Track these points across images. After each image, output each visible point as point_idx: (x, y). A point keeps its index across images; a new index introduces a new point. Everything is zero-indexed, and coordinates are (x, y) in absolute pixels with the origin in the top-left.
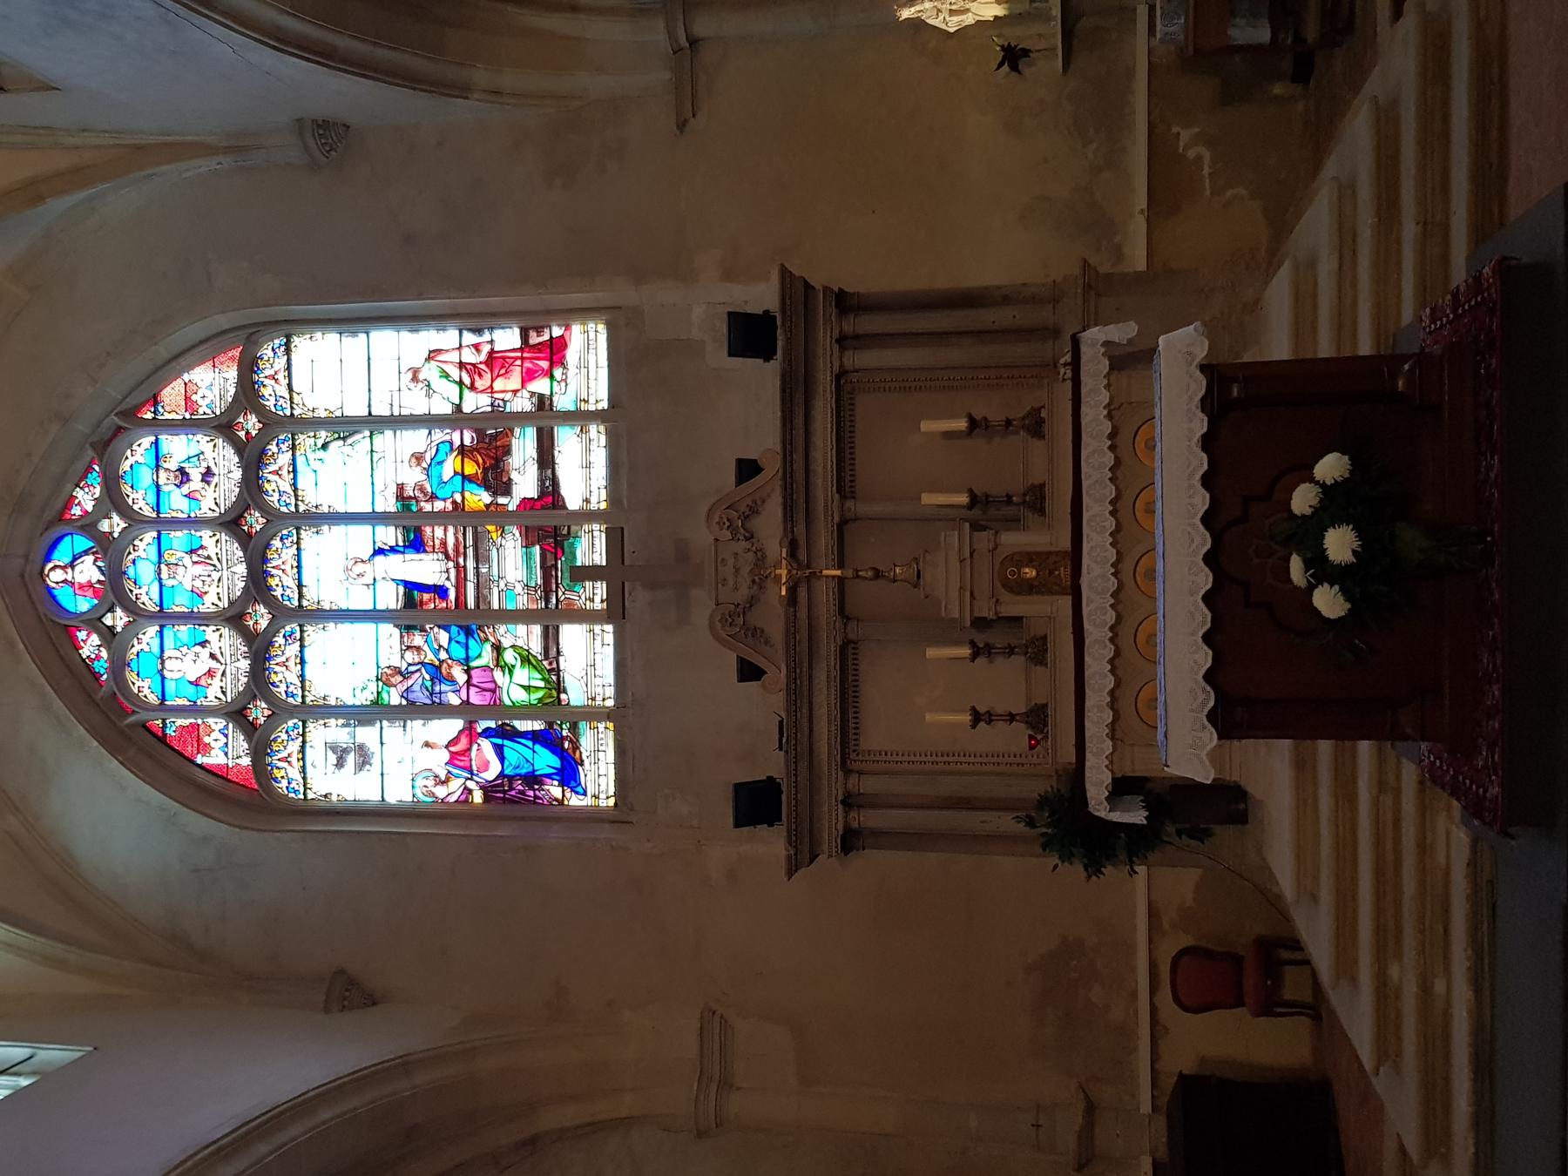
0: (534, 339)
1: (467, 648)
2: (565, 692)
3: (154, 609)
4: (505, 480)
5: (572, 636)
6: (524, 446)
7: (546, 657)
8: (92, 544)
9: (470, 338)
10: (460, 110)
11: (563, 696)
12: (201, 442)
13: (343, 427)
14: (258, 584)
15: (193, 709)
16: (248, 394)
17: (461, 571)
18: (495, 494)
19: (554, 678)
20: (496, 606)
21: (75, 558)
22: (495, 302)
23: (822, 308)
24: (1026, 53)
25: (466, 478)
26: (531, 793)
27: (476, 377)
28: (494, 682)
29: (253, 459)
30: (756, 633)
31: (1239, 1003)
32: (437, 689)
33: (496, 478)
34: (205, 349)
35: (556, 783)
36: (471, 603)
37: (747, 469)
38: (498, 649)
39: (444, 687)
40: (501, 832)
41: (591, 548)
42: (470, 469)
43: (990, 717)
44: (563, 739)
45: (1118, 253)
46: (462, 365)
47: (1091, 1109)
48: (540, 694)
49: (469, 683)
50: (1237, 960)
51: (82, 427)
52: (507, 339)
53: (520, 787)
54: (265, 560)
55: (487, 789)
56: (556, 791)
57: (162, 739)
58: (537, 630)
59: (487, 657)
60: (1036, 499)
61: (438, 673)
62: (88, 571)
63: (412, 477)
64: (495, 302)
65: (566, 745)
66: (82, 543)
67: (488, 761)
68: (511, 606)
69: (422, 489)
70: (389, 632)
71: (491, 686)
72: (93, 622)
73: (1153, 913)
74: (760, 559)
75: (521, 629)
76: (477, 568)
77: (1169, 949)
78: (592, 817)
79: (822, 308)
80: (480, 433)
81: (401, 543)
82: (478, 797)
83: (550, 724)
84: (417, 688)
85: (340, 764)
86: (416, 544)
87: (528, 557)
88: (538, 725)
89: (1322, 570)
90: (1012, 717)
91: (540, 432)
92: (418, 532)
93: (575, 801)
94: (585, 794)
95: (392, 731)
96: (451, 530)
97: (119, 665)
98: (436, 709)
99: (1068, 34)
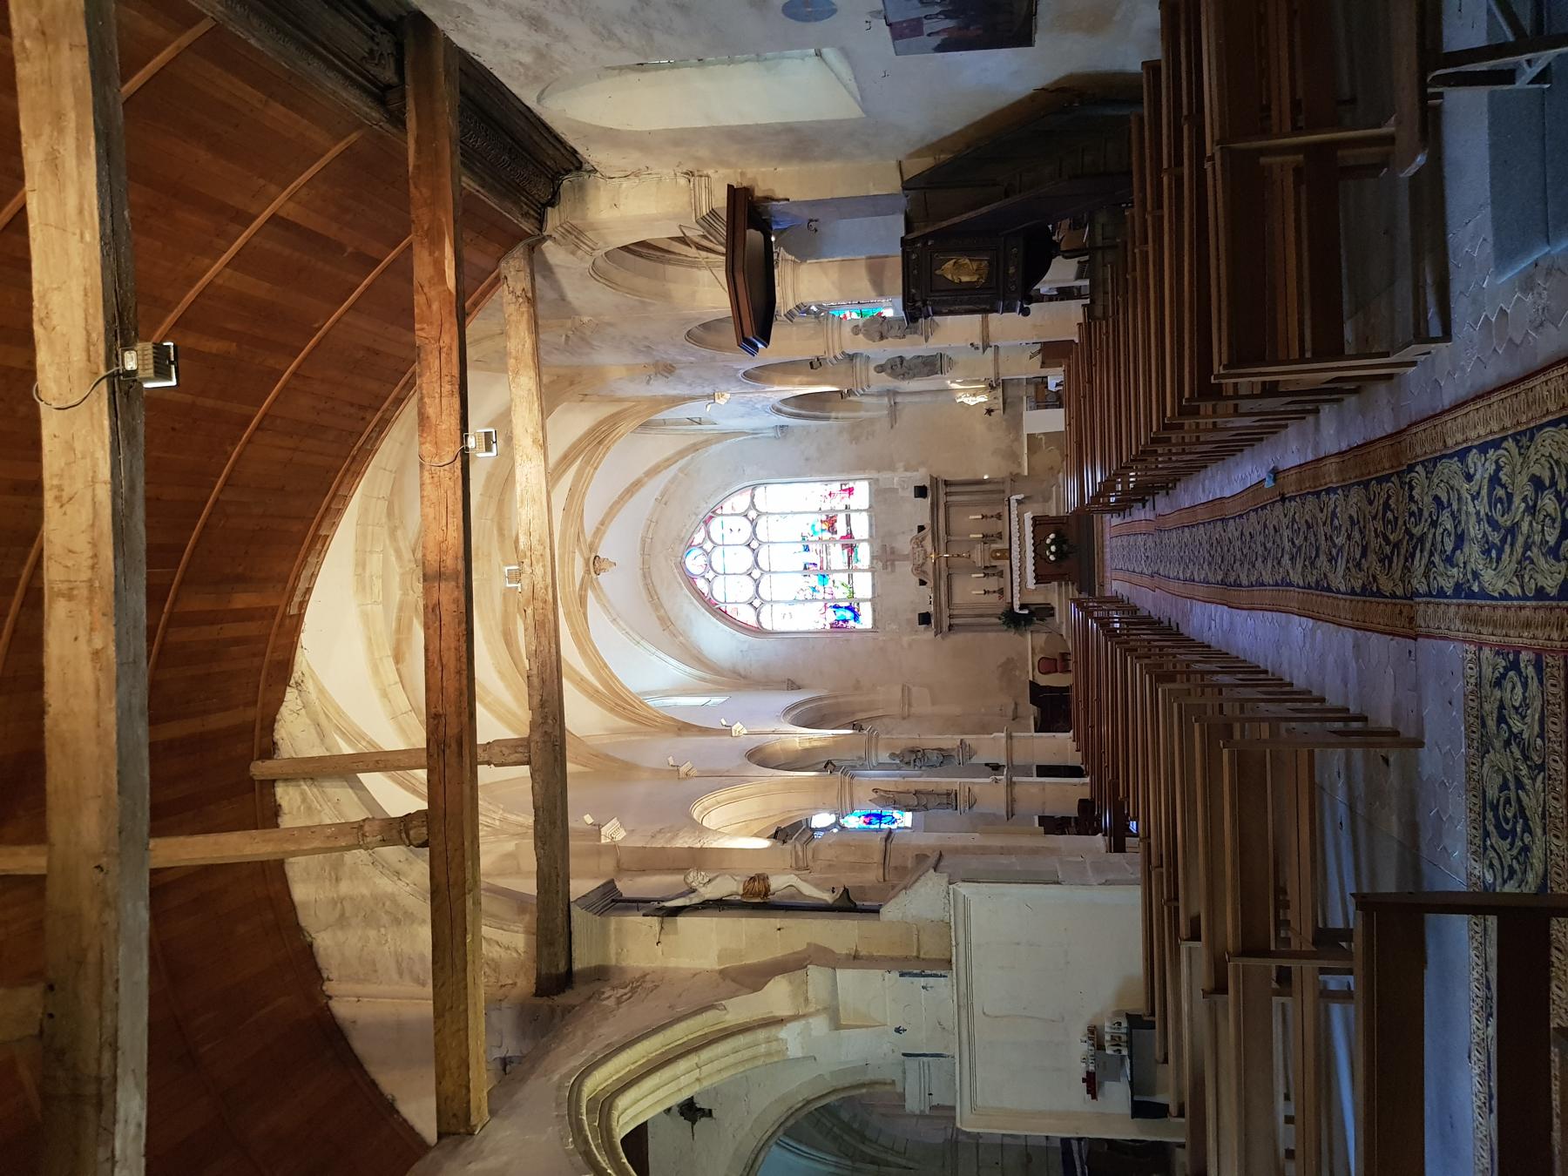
0: (844, 487)
6: (841, 519)
16: (753, 504)
22: (833, 478)
23: (941, 486)
24: (992, 411)
25: (823, 530)
29: (754, 523)
30: (924, 572)
31: (1056, 671)
33: (832, 529)
37: (921, 528)
40: (839, 635)
41: (864, 553)
42: (825, 527)
43: (989, 592)
45: (1020, 465)
47: (1016, 704)
50: (1056, 660)
51: (701, 517)
52: (835, 487)
56: (852, 623)
59: (831, 582)
60: (1000, 536)
62: (702, 560)
63: (807, 531)
64: (833, 478)
67: (831, 617)
70: (800, 576)
73: (1033, 649)
74: (925, 552)
75: (841, 574)
77: (1037, 659)
79: (941, 486)
82: (828, 627)
86: (807, 549)
88: (847, 604)
89: (1052, 553)
90: (994, 592)
93: (858, 626)
95: (798, 606)
99: (1004, 403)
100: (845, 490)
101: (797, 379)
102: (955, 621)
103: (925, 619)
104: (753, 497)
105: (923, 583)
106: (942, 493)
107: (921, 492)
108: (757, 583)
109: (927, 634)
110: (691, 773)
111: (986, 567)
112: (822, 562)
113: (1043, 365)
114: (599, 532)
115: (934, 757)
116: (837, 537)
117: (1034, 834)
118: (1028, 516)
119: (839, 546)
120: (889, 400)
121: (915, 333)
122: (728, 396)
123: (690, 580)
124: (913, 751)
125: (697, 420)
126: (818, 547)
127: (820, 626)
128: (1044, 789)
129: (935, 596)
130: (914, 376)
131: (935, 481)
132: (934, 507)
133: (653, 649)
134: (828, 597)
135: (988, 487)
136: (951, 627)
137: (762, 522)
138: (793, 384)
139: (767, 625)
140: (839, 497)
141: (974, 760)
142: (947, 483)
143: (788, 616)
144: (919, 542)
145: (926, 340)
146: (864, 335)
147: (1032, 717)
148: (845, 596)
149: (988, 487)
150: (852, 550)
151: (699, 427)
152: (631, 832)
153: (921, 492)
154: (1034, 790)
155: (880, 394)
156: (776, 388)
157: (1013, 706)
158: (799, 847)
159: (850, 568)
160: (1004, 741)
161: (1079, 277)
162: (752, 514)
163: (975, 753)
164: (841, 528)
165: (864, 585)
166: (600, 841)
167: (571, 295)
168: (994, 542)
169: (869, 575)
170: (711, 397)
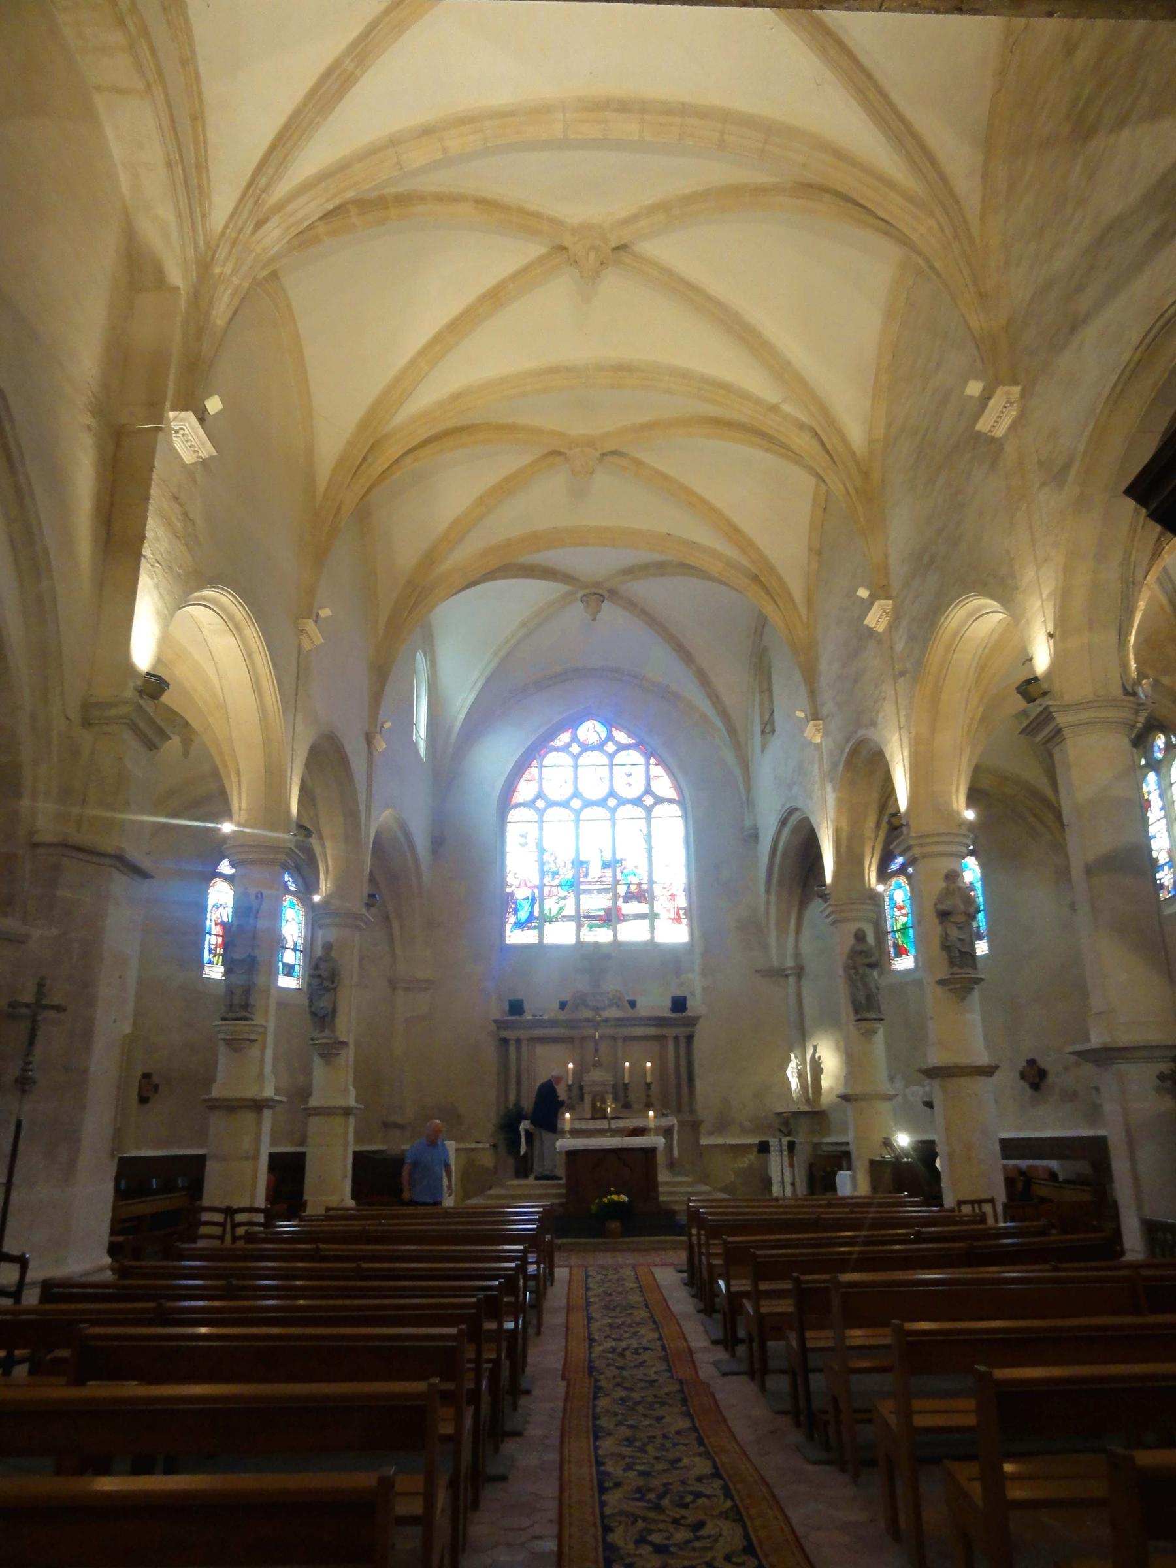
0: (681, 912)
1: (565, 885)
2: (550, 924)
3: (579, 763)
4: (629, 900)
5: (572, 925)
6: (643, 908)
7: (562, 917)
8: (603, 739)
9: (682, 887)
10: (762, 889)
11: (548, 923)
12: (643, 782)
13: (648, 838)
14: (588, 804)
15: (541, 779)
16: (659, 800)
17: (594, 883)
18: (624, 897)
19: (554, 919)
20: (581, 896)
21: (598, 732)
26: (511, 910)
27: (667, 889)
28: (553, 896)
29: (637, 802)
32: (550, 873)
33: (629, 897)
34: (677, 786)
35: (515, 920)
36: (582, 887)
38: (565, 898)
39: (550, 876)
41: (603, 936)
42: (633, 887)
44: (531, 923)
45: (711, 1134)
46: (671, 884)
47: (401, 1127)
48: (548, 914)
49: (552, 886)
52: (682, 901)
53: (513, 906)
54: (598, 806)
55: (512, 894)
57: (530, 766)
58: (573, 913)
59: (563, 894)
61: (556, 874)
62: (593, 739)
63: (628, 865)
64: (694, 898)
65: (529, 924)
66: (604, 735)
67: (521, 894)
68: (581, 902)
69: (625, 868)
70: (572, 856)
71: (551, 895)
72: (574, 739)
74: (604, 1009)
76: (595, 890)
78: (502, 935)
80: (646, 891)
81: (605, 860)
82: (508, 890)
83: (537, 918)
84: (550, 866)
85: (522, 836)
86: (606, 865)
87: (600, 910)
88: (536, 914)
91: (647, 914)
92: (609, 866)
93: (508, 927)
94: (511, 932)
95: (535, 856)
96: (610, 879)
97: (557, 749)
98: (543, 874)
100: (678, 914)
101: (845, 825)
102: (512, 1049)
103: (516, 1008)
104: (670, 801)
105: (563, 1005)
106: (681, 1031)
107: (679, 1004)
108: (565, 804)
109: (497, 1010)
110: (304, 638)
111: (581, 1088)
112: (590, 883)
113: (874, 1164)
114: (631, 605)
115: (324, 1003)
116: (620, 903)
117: (118, 1134)
118: (660, 1141)
119: (609, 904)
120: (791, 968)
121: (952, 964)
122: (817, 740)
123: (572, 723)
124: (334, 975)
125: (768, 729)
126: (608, 880)
127: (510, 879)
128: (247, 1158)
129: (546, 1021)
130: (851, 981)
131: (693, 1022)
132: (660, 1022)
133: (487, 673)
134: (546, 890)
135: (685, 1091)
136: (505, 1042)
137: (639, 812)
138: (837, 821)
139: (513, 815)
140: (670, 905)
141: (317, 1060)
142: (690, 1038)
143: (523, 840)
144: (616, 1002)
145: (942, 982)
146: (947, 889)
147: (385, 1147)
148: (547, 912)
149: (685, 1091)
150: (605, 921)
151: (758, 728)
152: (189, 471)
153: (679, 1004)
154: (247, 1143)
155: (797, 955)
156: (831, 797)
157: (400, 1120)
158: (123, 710)
159: (579, 919)
160: (342, 1103)
161: (1151, 1229)
162: (649, 801)
163: (328, 1063)
164: (629, 908)
165: (560, 935)
166: (173, 409)
167: (1090, 333)
168: (615, 1100)
169: (571, 941)
170: (815, 716)
